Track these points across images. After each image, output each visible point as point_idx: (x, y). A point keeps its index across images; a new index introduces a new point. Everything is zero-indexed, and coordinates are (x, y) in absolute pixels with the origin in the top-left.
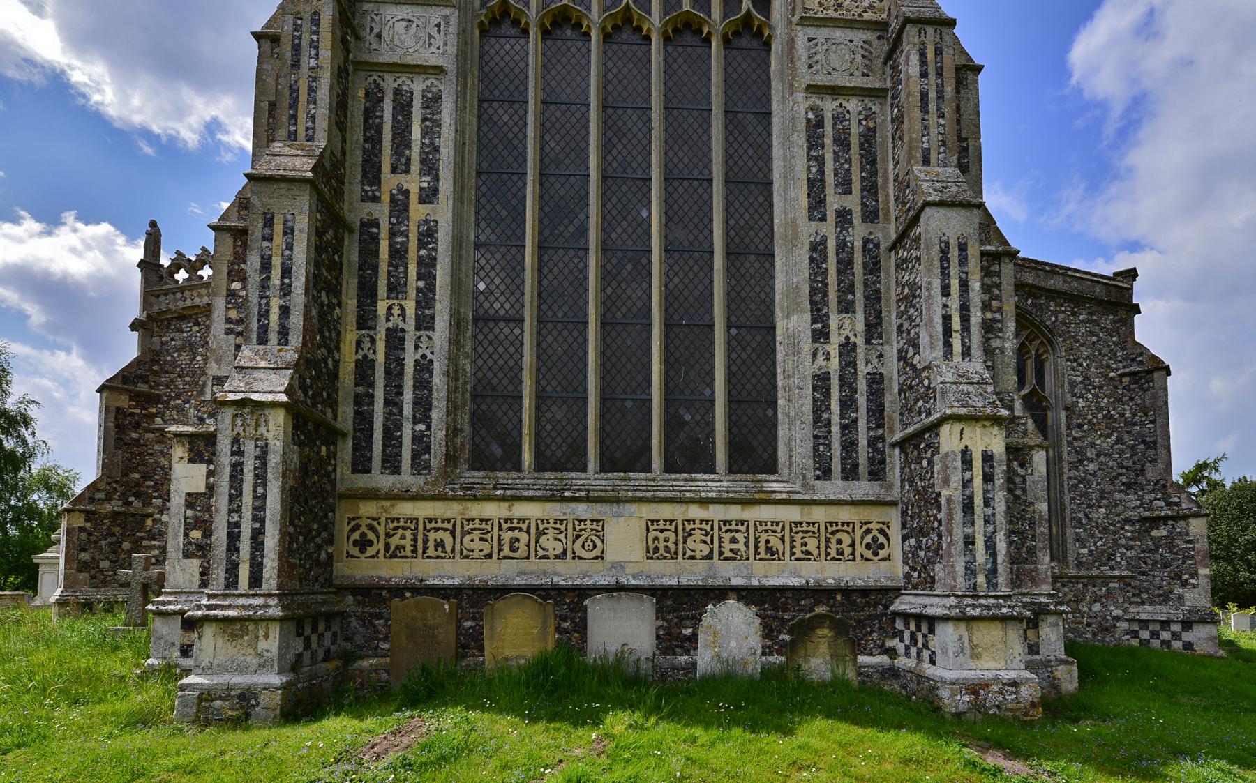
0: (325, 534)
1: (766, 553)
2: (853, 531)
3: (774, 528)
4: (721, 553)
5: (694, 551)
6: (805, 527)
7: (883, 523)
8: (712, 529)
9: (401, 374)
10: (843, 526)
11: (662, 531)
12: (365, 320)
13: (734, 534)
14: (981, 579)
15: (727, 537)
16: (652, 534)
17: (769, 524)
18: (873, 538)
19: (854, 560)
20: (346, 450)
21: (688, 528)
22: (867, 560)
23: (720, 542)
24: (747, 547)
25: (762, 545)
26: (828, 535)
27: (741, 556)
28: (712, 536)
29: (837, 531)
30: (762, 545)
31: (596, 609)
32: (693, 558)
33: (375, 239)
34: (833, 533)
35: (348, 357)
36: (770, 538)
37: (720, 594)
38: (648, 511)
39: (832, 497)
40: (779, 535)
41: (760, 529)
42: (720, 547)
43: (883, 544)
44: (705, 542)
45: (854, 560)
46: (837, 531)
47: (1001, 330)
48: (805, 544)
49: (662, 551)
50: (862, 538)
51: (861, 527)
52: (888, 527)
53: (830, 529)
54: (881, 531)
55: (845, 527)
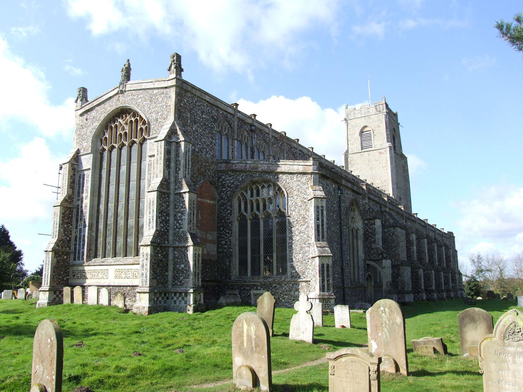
0: (66, 274)
9: (81, 238)
12: (76, 228)
14: (144, 283)
15: (128, 273)
20: (72, 256)
21: (122, 271)
25: (134, 275)
32: (122, 278)
33: (79, 209)
47: (185, 213)
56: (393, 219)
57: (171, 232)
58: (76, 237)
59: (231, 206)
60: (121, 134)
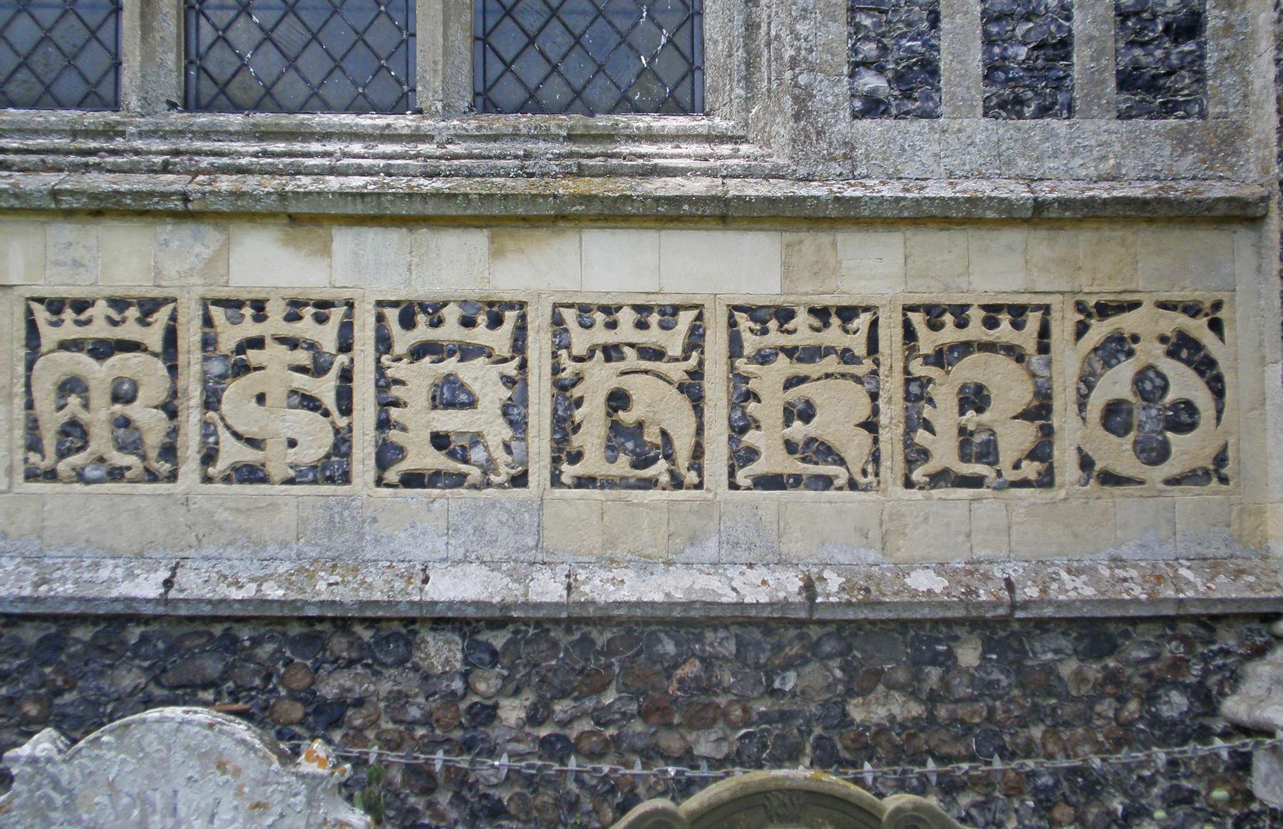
1: (612, 450)
2: (1044, 349)
3: (653, 336)
4: (386, 455)
5: (253, 443)
6: (803, 332)
7: (1192, 310)
8: (345, 346)
10: (991, 323)
11: (102, 350)
13: (451, 365)
16: (55, 366)
17: (627, 317)
18: (1140, 378)
19: (1046, 480)
21: (229, 336)
22: (1109, 479)
23: (386, 404)
24: (519, 425)
25: (592, 415)
26: (918, 368)
27: (489, 467)
28: (346, 375)
29: (966, 348)
30: (592, 415)
32: (251, 474)
34: (940, 358)
36: (629, 383)
39: (937, 190)
40: (677, 371)
41: (580, 341)
42: (383, 424)
43: (1189, 407)
44: (310, 403)
45: (1046, 480)
46: (966, 348)
48: (807, 414)
49: (101, 441)
50: (1087, 381)
51: (1082, 329)
52: (1216, 326)
53: (928, 341)
54: (1182, 346)
55: (1004, 332)
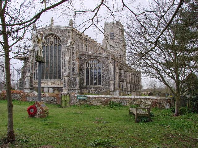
20: (34, 78)
31: (45, 88)
35: (34, 72)
37: (50, 87)
38: (51, 82)
56: (126, 69)
57: (71, 73)
58: (35, 72)
59: (84, 65)
60: (51, 42)
